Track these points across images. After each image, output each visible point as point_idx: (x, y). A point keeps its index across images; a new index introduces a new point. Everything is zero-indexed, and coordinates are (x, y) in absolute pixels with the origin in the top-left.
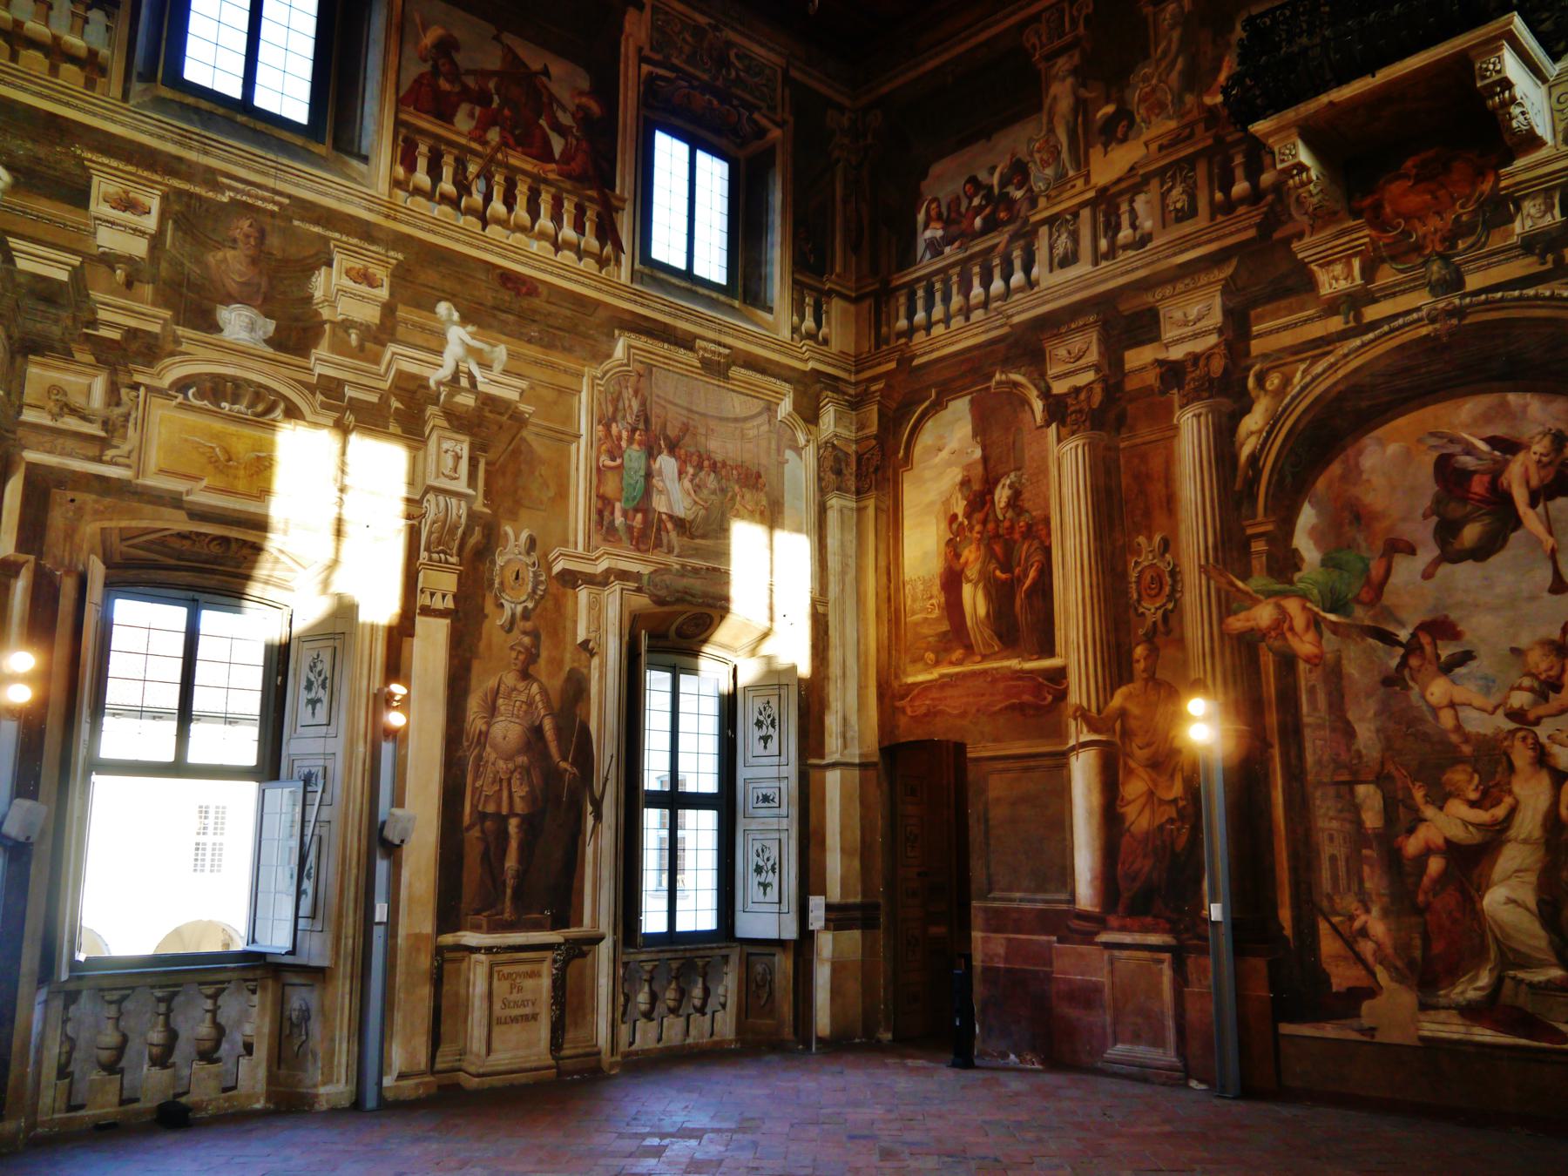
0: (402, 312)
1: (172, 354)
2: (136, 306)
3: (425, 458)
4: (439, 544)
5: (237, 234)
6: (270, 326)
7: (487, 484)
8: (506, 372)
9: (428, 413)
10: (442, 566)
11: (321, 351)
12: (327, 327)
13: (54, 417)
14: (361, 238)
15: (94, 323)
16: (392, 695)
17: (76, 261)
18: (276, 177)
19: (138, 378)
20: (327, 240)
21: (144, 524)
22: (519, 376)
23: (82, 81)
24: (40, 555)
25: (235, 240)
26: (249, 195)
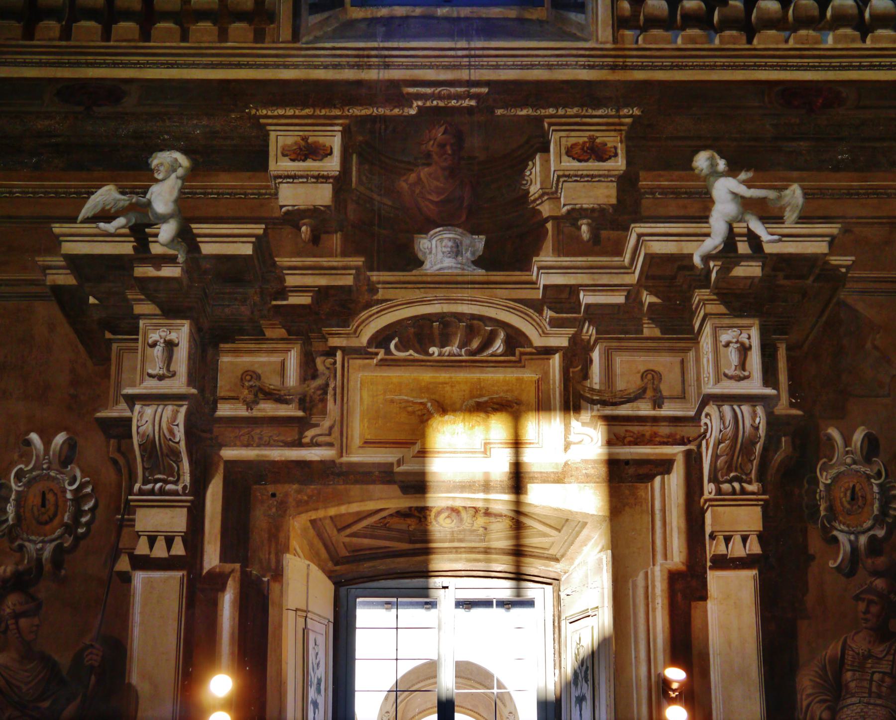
0: (645, 182)
1: (368, 305)
2: (324, 261)
3: (698, 360)
4: (730, 470)
5: (431, 146)
6: (480, 242)
7: (791, 377)
8: (803, 219)
9: (696, 300)
10: (739, 498)
11: (546, 257)
12: (549, 225)
13: (250, 406)
14: (582, 106)
15: (283, 292)
16: (665, 684)
17: (259, 229)
18: (469, 67)
19: (334, 342)
20: (540, 120)
21: (355, 508)
22: (826, 219)
23: (251, 36)
24: (245, 562)
25: (428, 155)
26: (440, 97)
